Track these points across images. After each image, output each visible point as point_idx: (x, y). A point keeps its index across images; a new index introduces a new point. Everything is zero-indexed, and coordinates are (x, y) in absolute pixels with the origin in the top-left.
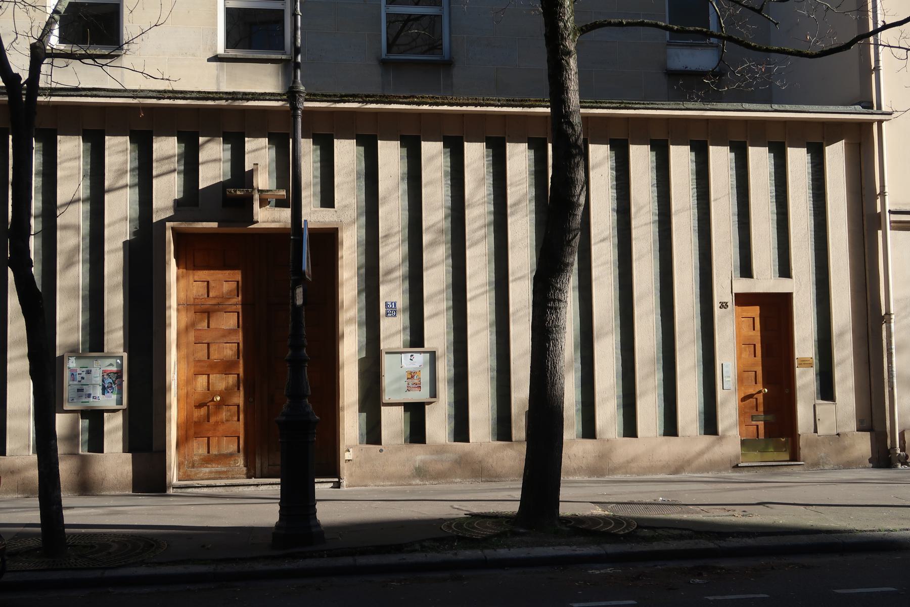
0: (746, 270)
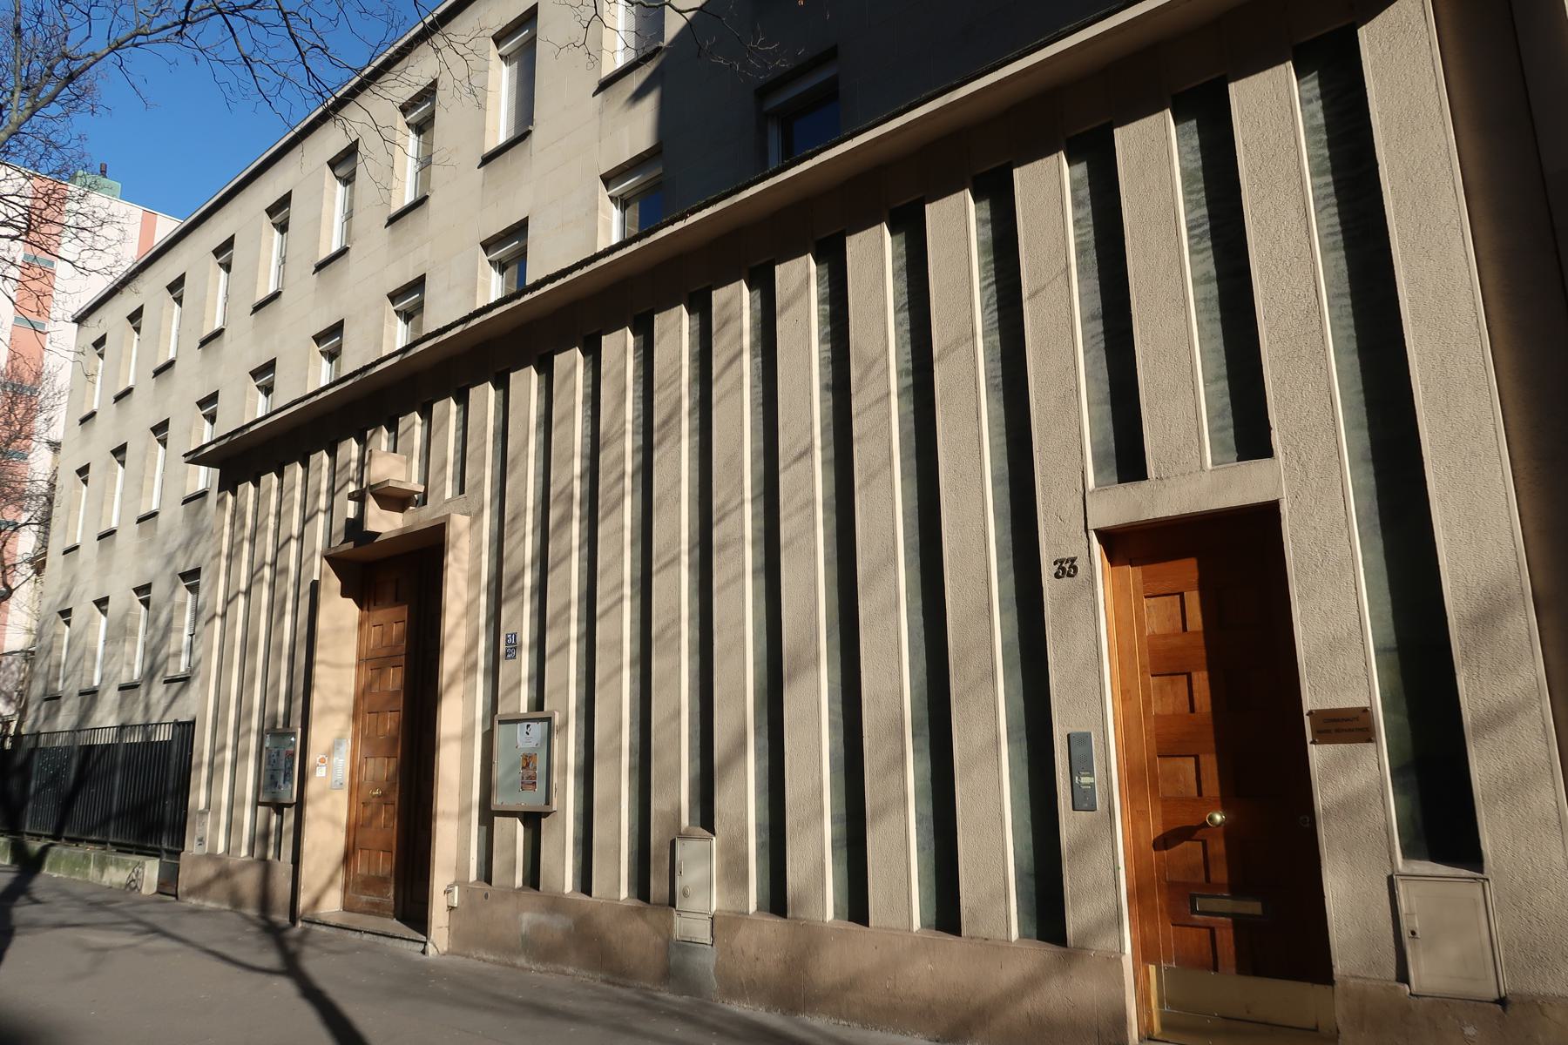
0: (1128, 459)
